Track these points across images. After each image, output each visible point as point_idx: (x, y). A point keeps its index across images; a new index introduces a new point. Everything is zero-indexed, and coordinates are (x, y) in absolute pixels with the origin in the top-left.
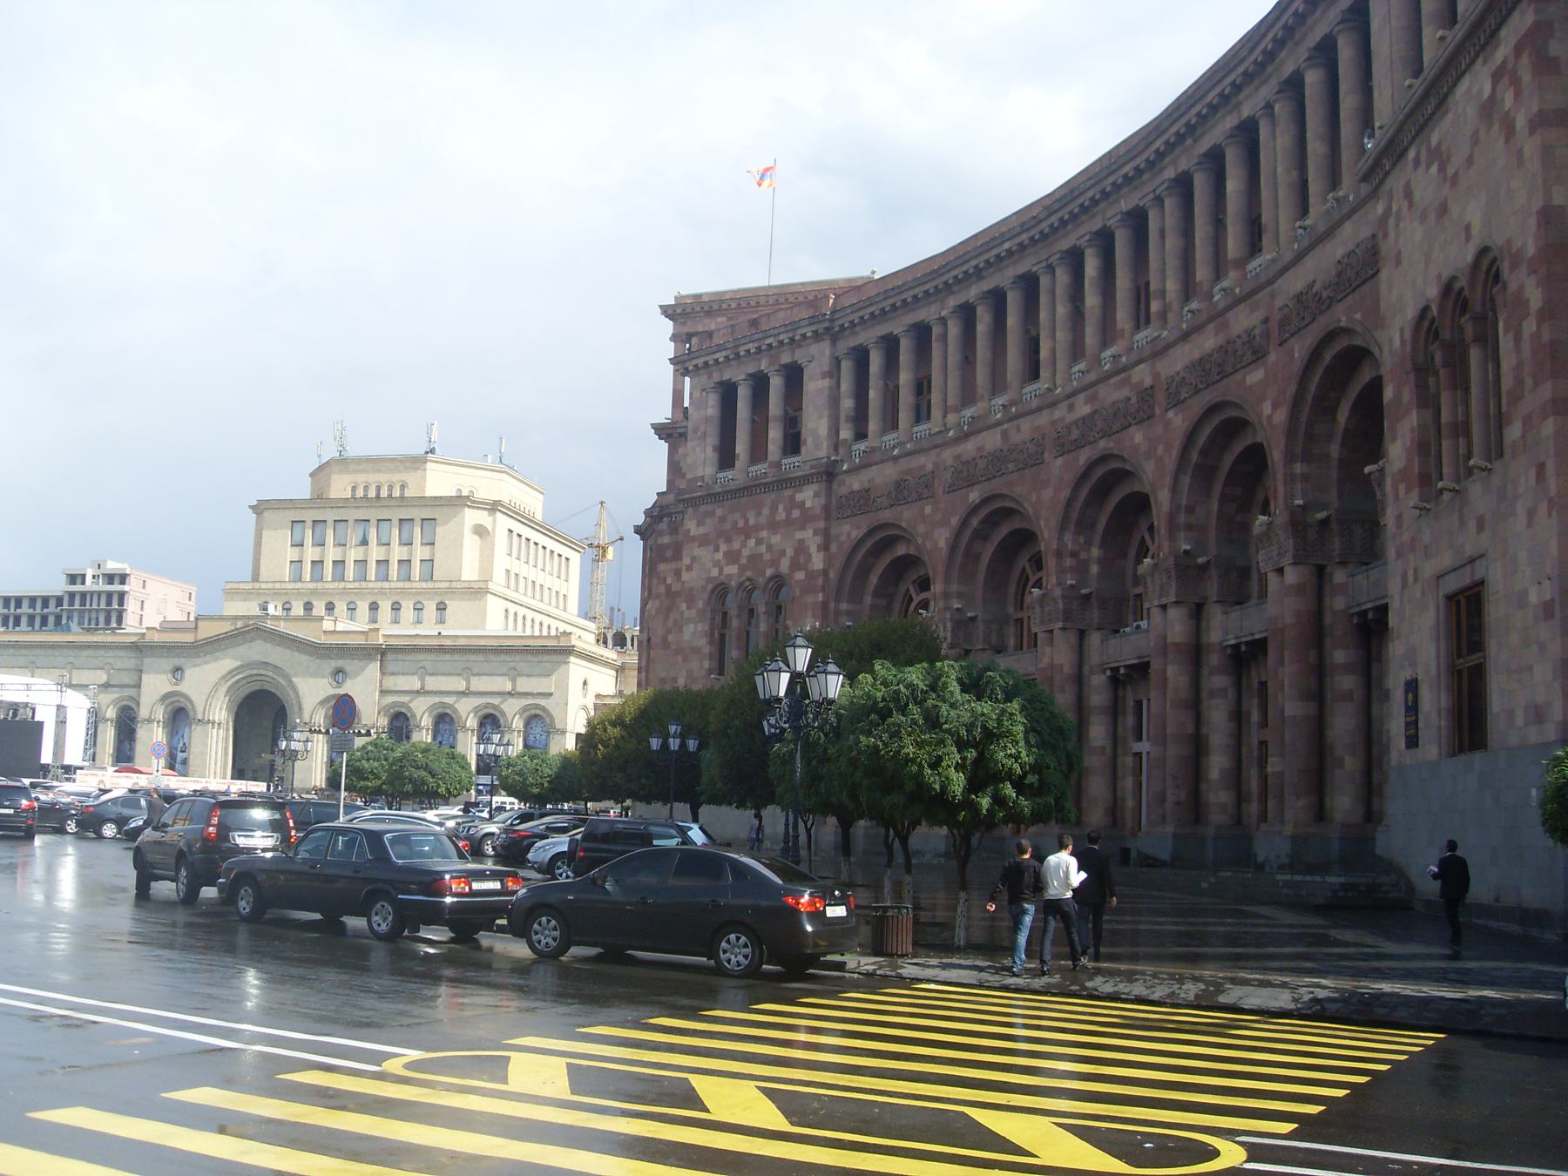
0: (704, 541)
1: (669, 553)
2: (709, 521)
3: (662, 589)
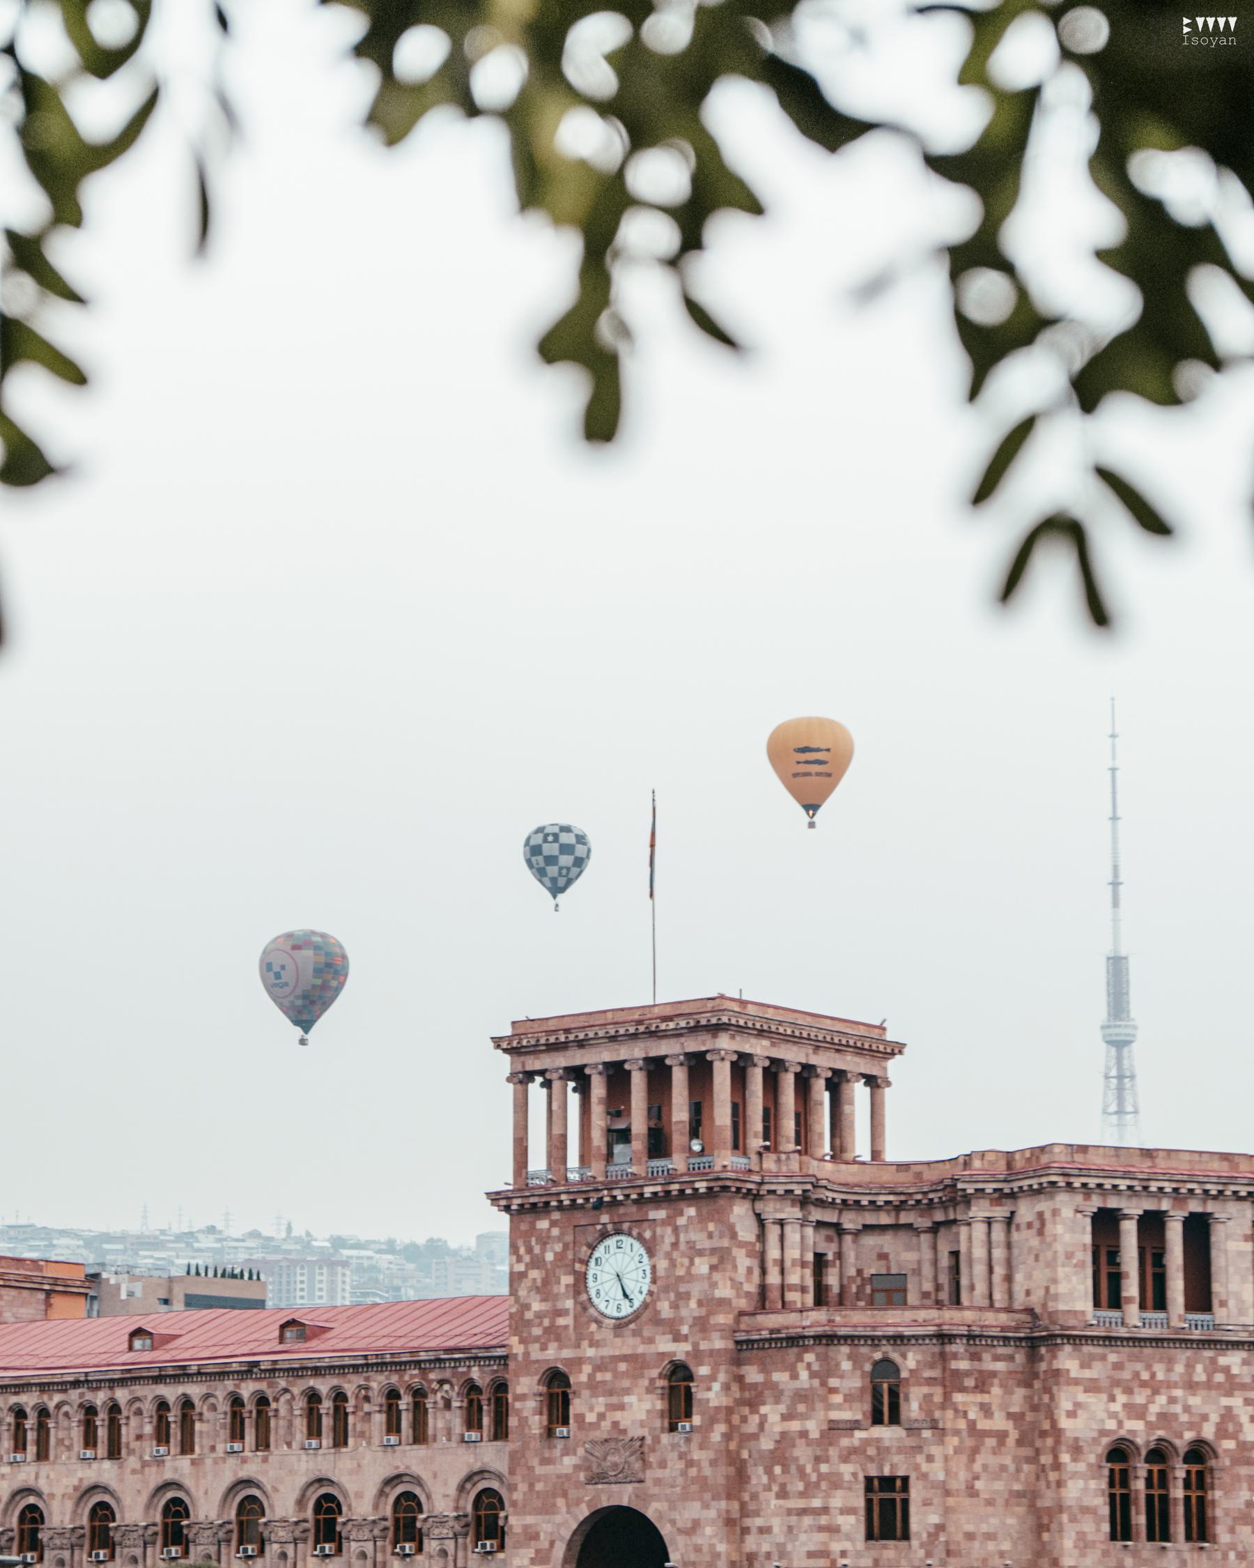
0: (1092, 1387)
1: (969, 1382)
2: (1097, 1365)
3: (962, 1424)
